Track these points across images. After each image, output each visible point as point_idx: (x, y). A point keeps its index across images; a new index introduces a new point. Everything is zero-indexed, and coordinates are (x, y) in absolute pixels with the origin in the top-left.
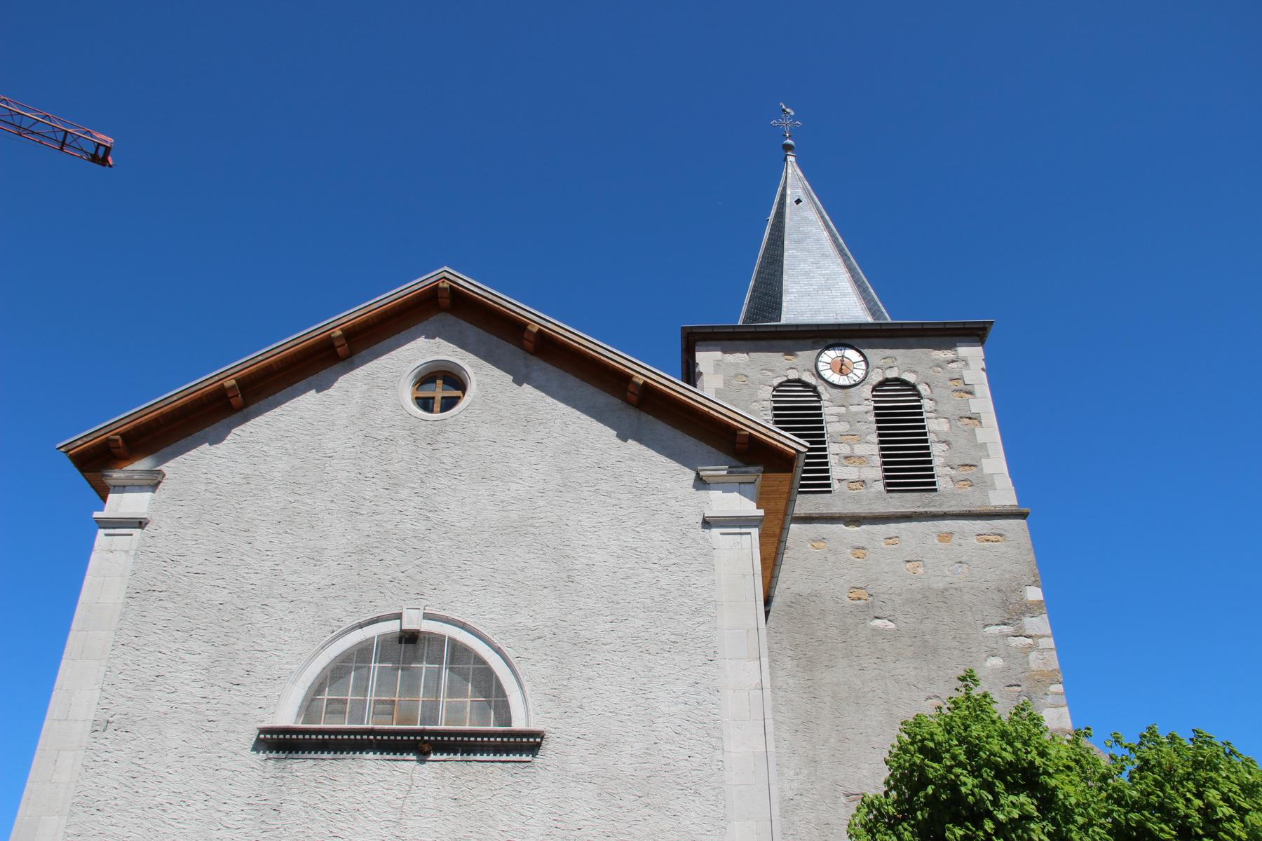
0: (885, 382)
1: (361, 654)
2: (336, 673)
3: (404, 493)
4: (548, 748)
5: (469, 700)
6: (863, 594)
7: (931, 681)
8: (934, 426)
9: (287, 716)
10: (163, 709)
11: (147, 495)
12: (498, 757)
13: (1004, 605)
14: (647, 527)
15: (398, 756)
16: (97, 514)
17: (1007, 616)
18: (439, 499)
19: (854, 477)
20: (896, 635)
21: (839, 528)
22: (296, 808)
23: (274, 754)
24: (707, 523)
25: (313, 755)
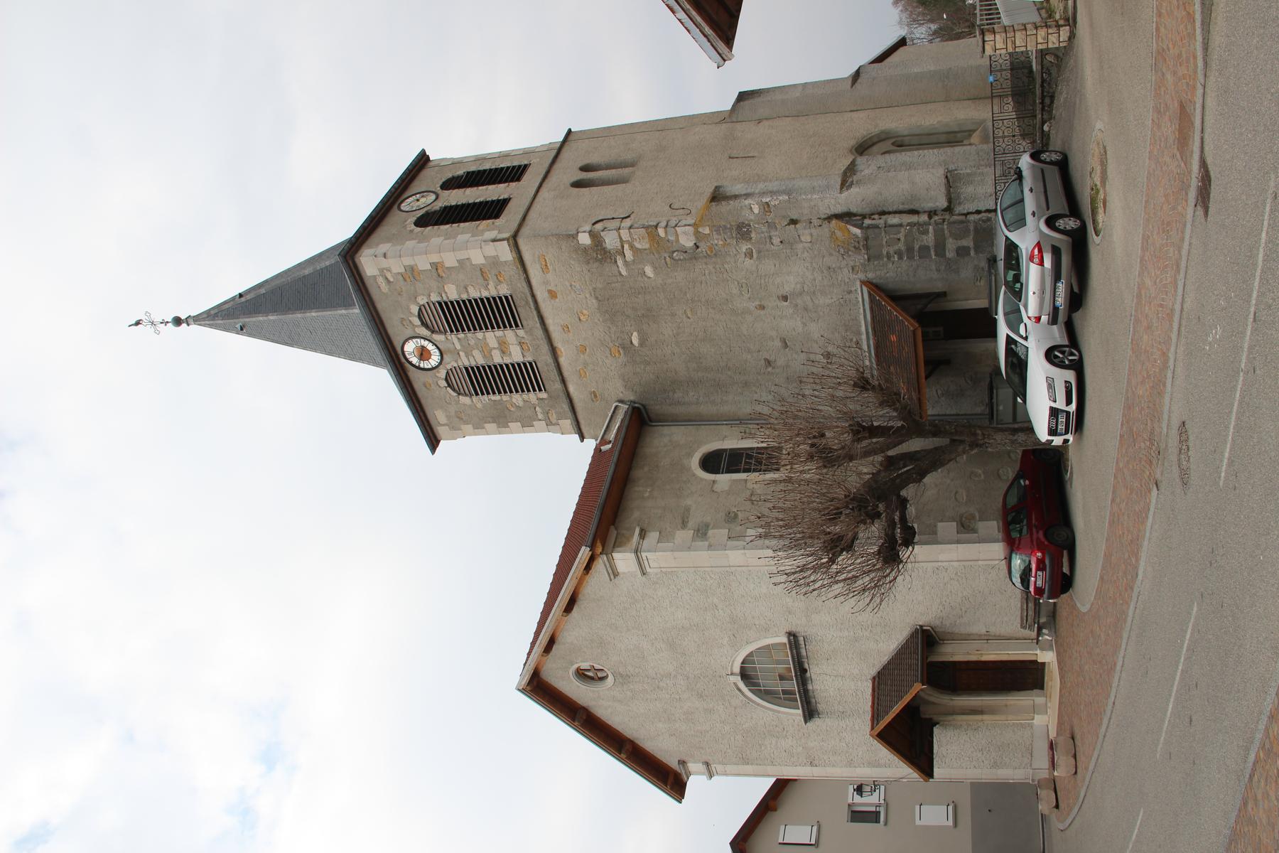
0: (424, 324)
1: (758, 693)
2: (767, 695)
3: (661, 684)
7: (673, 315)
8: (452, 293)
13: (601, 261)
19: (518, 348)
21: (562, 360)
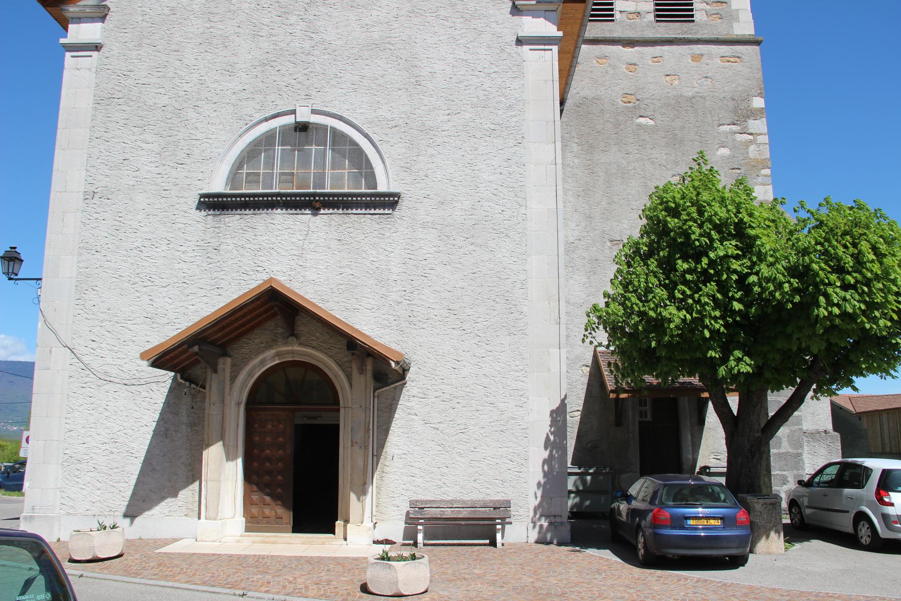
1: (268, 140)
2: (251, 153)
3: (293, 19)
4: (403, 204)
5: (346, 171)
6: (632, 99)
7: (676, 163)
9: (218, 185)
10: (131, 183)
11: (100, 24)
12: (368, 211)
13: (735, 110)
14: (475, 44)
15: (298, 211)
16: (62, 41)
17: (736, 118)
18: (319, 24)
19: (632, 9)
20: (654, 130)
21: (618, 48)
22: (230, 248)
23: (211, 212)
24: (520, 42)
25: (239, 211)
